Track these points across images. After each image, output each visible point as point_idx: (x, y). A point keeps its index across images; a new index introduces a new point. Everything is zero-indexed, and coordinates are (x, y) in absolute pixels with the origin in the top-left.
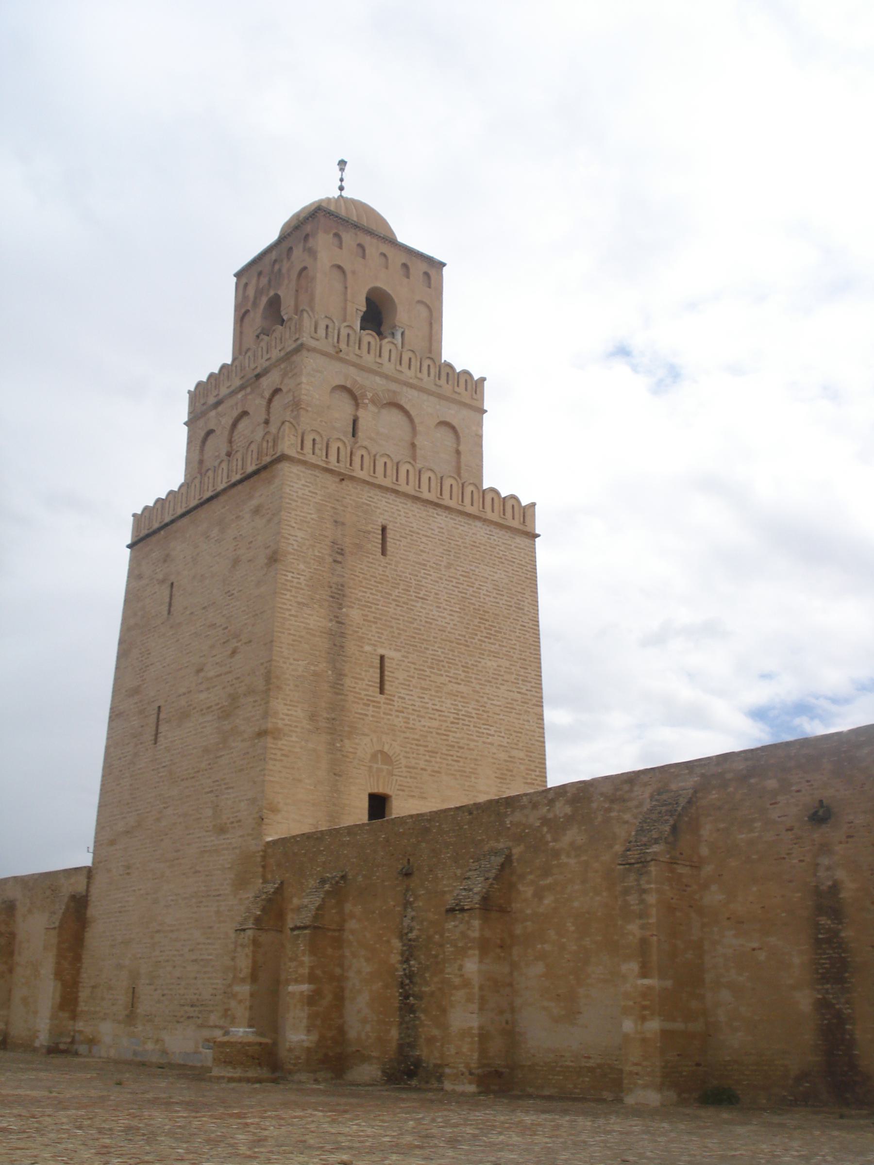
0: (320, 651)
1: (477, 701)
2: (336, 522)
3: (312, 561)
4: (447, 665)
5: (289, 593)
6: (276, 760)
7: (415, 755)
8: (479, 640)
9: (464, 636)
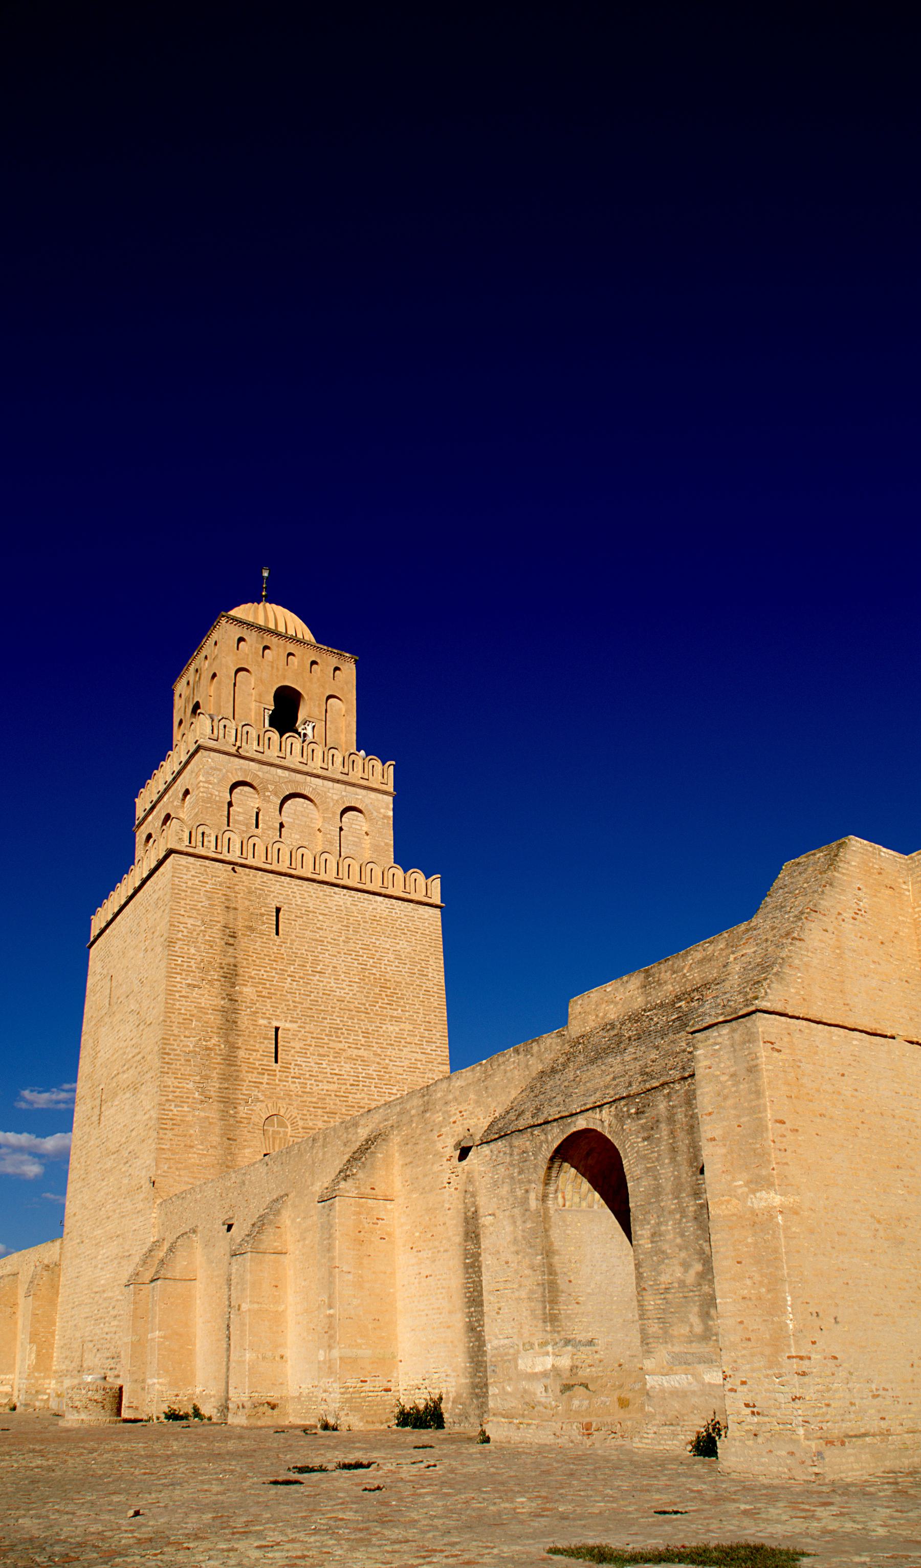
0: (212, 1027)
1: (378, 1063)
2: (227, 907)
3: (203, 946)
4: (346, 1032)
5: (179, 976)
6: (166, 1129)
7: (312, 1117)
8: (380, 1007)
9: (364, 1004)
